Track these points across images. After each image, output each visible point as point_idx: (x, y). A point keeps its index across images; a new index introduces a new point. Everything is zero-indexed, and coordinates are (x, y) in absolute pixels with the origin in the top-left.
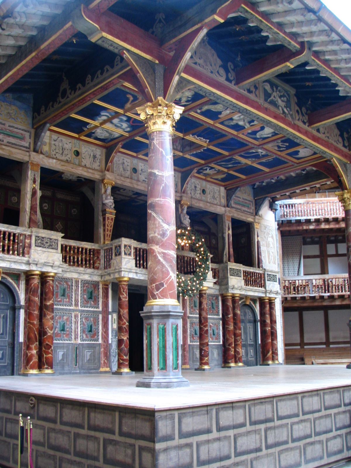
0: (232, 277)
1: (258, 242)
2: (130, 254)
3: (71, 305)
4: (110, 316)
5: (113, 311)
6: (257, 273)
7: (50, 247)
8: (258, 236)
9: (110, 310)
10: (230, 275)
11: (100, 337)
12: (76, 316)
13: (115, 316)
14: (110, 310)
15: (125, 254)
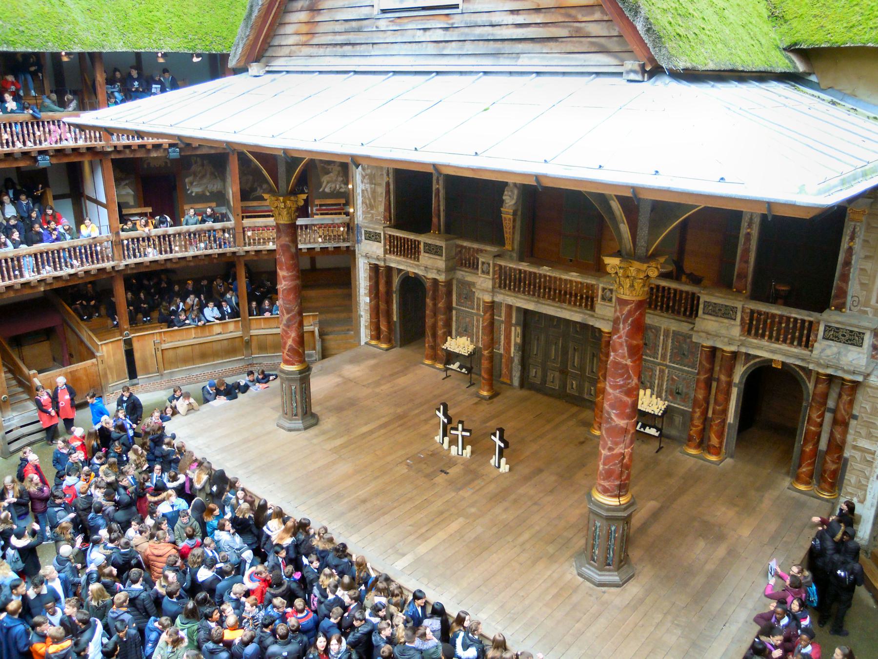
0: (706, 317)
1: (850, 250)
2: (488, 273)
3: (473, 309)
4: (513, 328)
5: (517, 324)
6: (796, 320)
7: (436, 253)
8: (852, 239)
9: (514, 322)
10: (704, 313)
11: (502, 348)
12: (478, 321)
13: (519, 330)
14: (514, 322)
15: (483, 272)
